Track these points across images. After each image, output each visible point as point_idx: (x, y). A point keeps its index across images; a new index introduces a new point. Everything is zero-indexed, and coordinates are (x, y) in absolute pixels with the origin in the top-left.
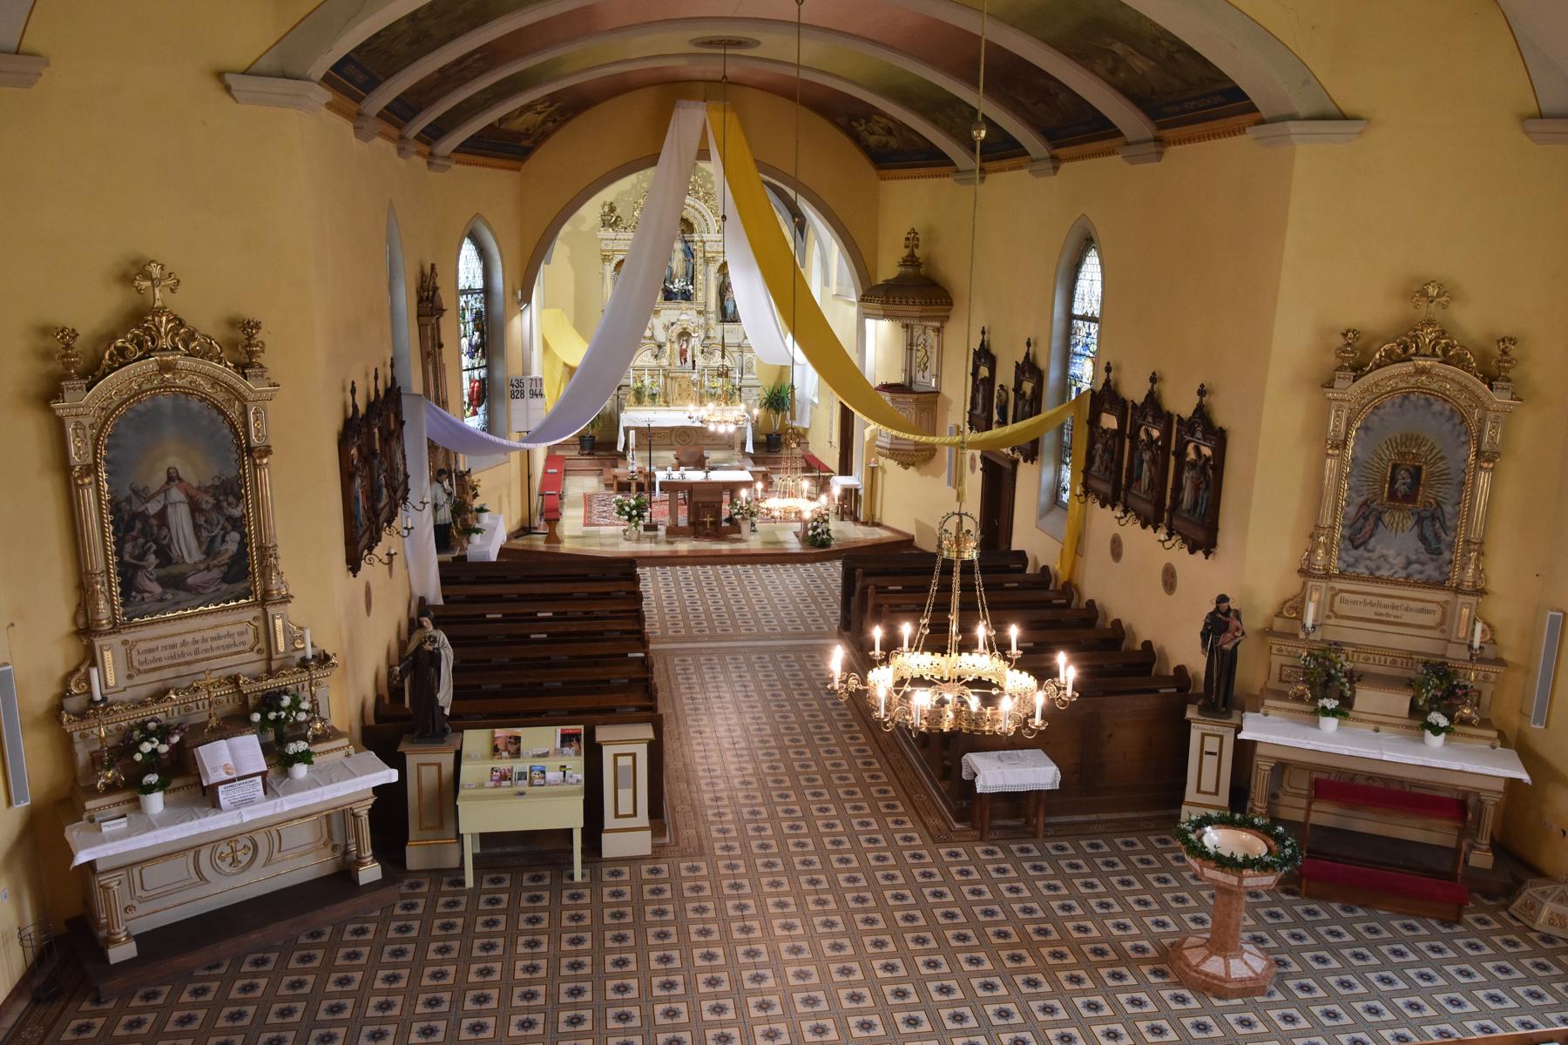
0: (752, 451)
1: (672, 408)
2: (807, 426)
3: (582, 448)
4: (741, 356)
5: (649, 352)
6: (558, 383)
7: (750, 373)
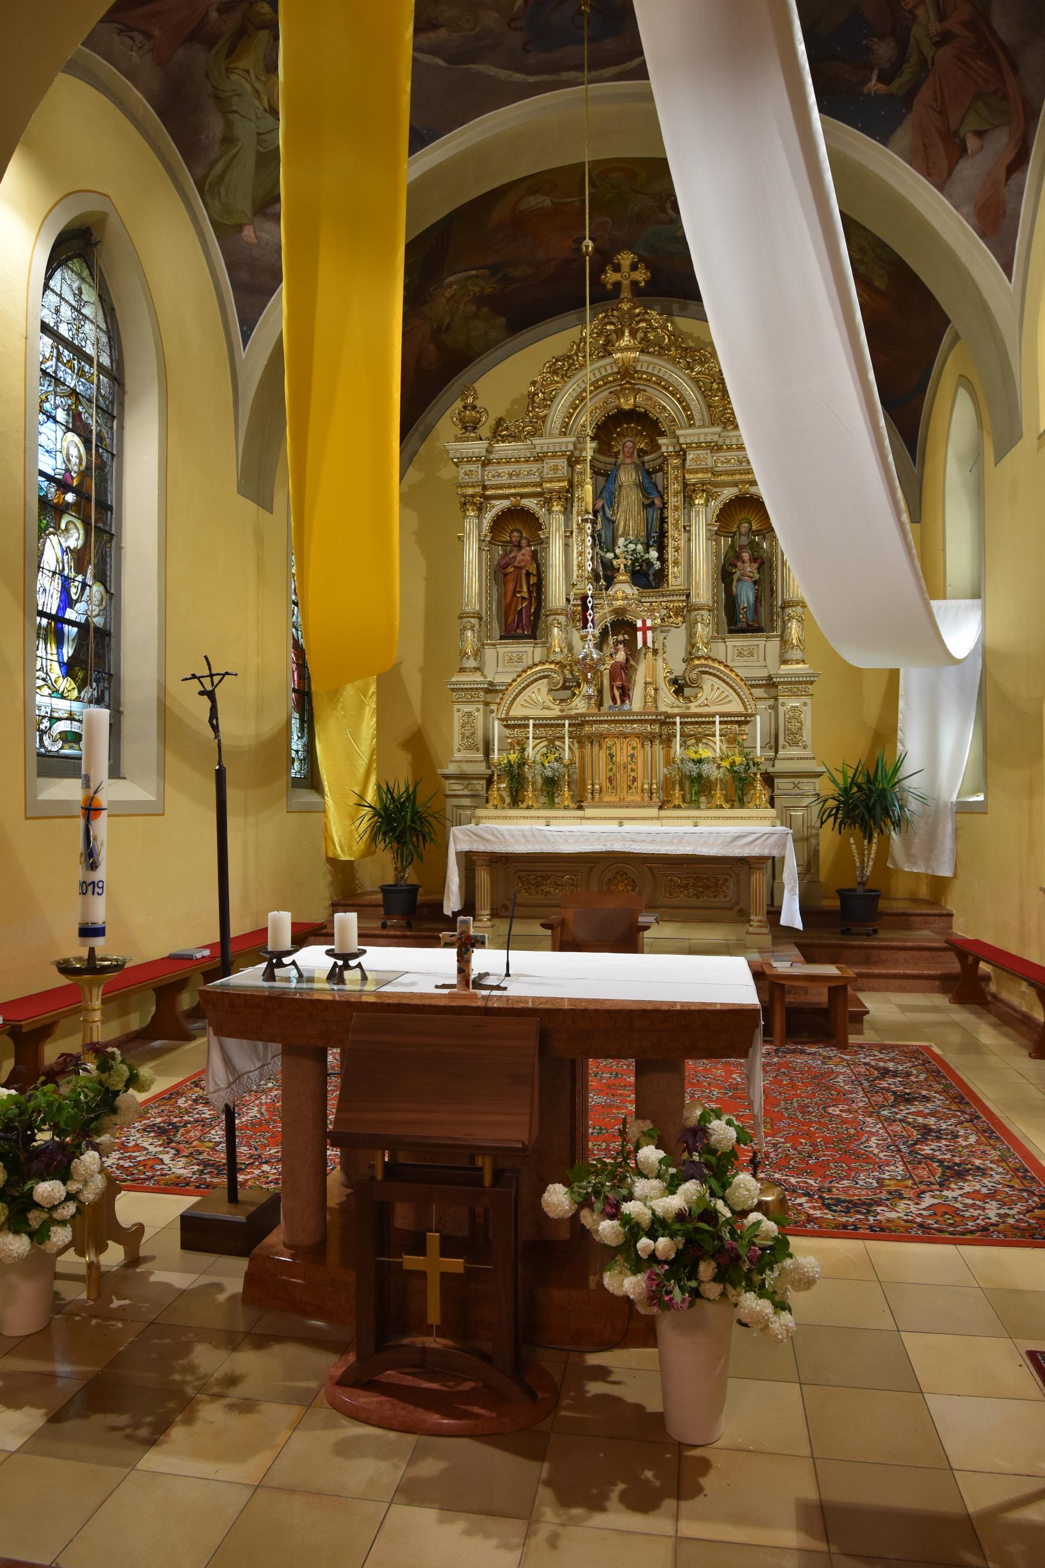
0: (799, 925)
1: (589, 812)
2: (946, 872)
3: (388, 913)
4: (774, 708)
5: (543, 685)
6: (362, 771)
7: (795, 744)
